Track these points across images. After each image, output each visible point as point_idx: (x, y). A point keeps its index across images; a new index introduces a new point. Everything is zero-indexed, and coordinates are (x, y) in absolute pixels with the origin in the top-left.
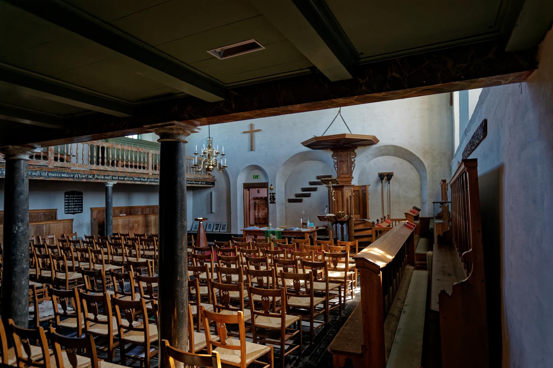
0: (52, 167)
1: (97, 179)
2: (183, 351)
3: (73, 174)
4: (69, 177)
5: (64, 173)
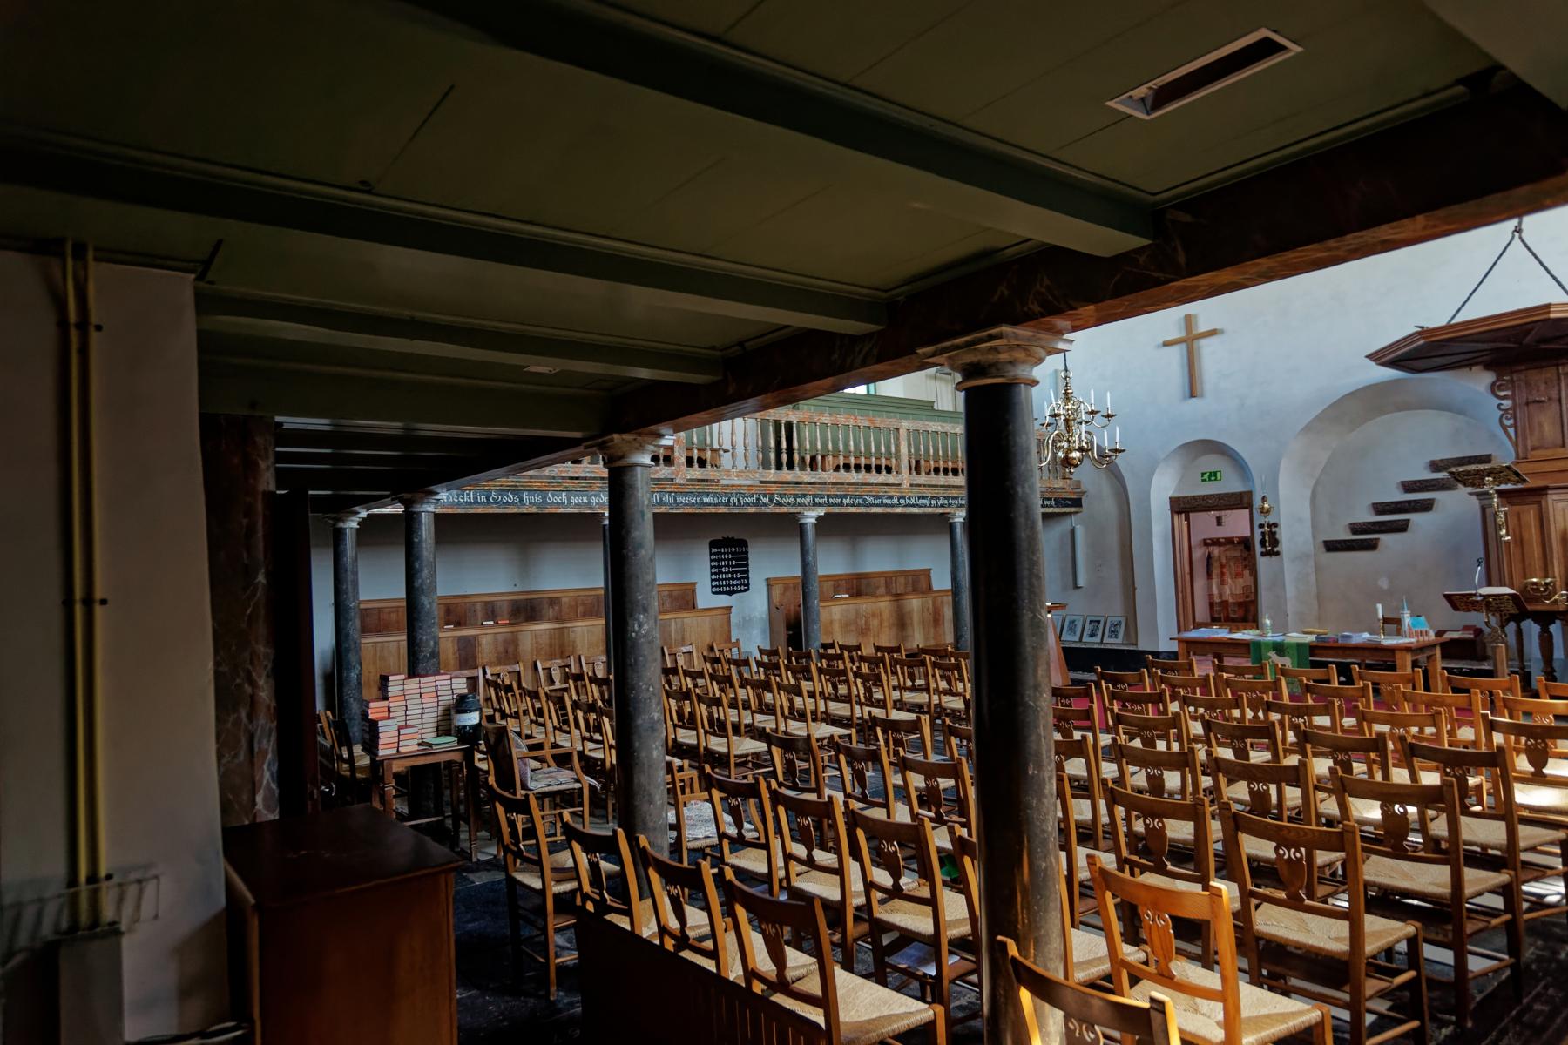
0: (682, 482)
1: (779, 504)
2: (1050, 975)
3: (726, 495)
4: (718, 504)
5: (708, 494)
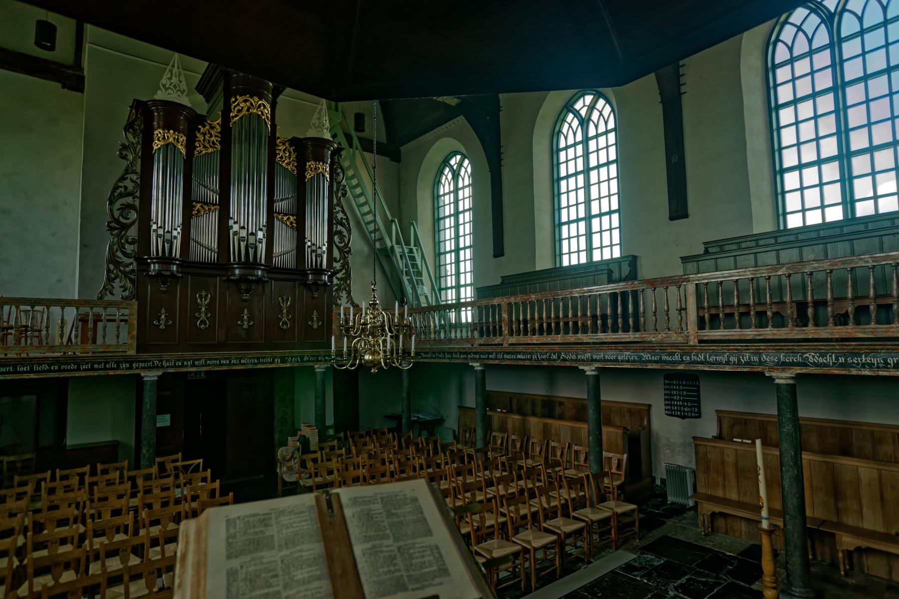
1: (565, 360)
3: (530, 353)
5: (519, 353)
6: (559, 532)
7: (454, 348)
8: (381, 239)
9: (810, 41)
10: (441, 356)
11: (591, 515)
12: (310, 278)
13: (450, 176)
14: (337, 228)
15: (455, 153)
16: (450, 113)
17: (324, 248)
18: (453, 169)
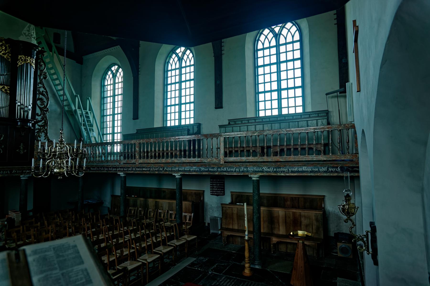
1: (166, 171)
5: (144, 168)
6: (161, 253)
7: (110, 165)
8: (69, 105)
9: (270, 43)
10: (102, 169)
11: (176, 243)
12: (19, 124)
13: (111, 76)
14: (39, 96)
15: (114, 64)
16: (112, 44)
17: (30, 107)
18: (113, 72)
